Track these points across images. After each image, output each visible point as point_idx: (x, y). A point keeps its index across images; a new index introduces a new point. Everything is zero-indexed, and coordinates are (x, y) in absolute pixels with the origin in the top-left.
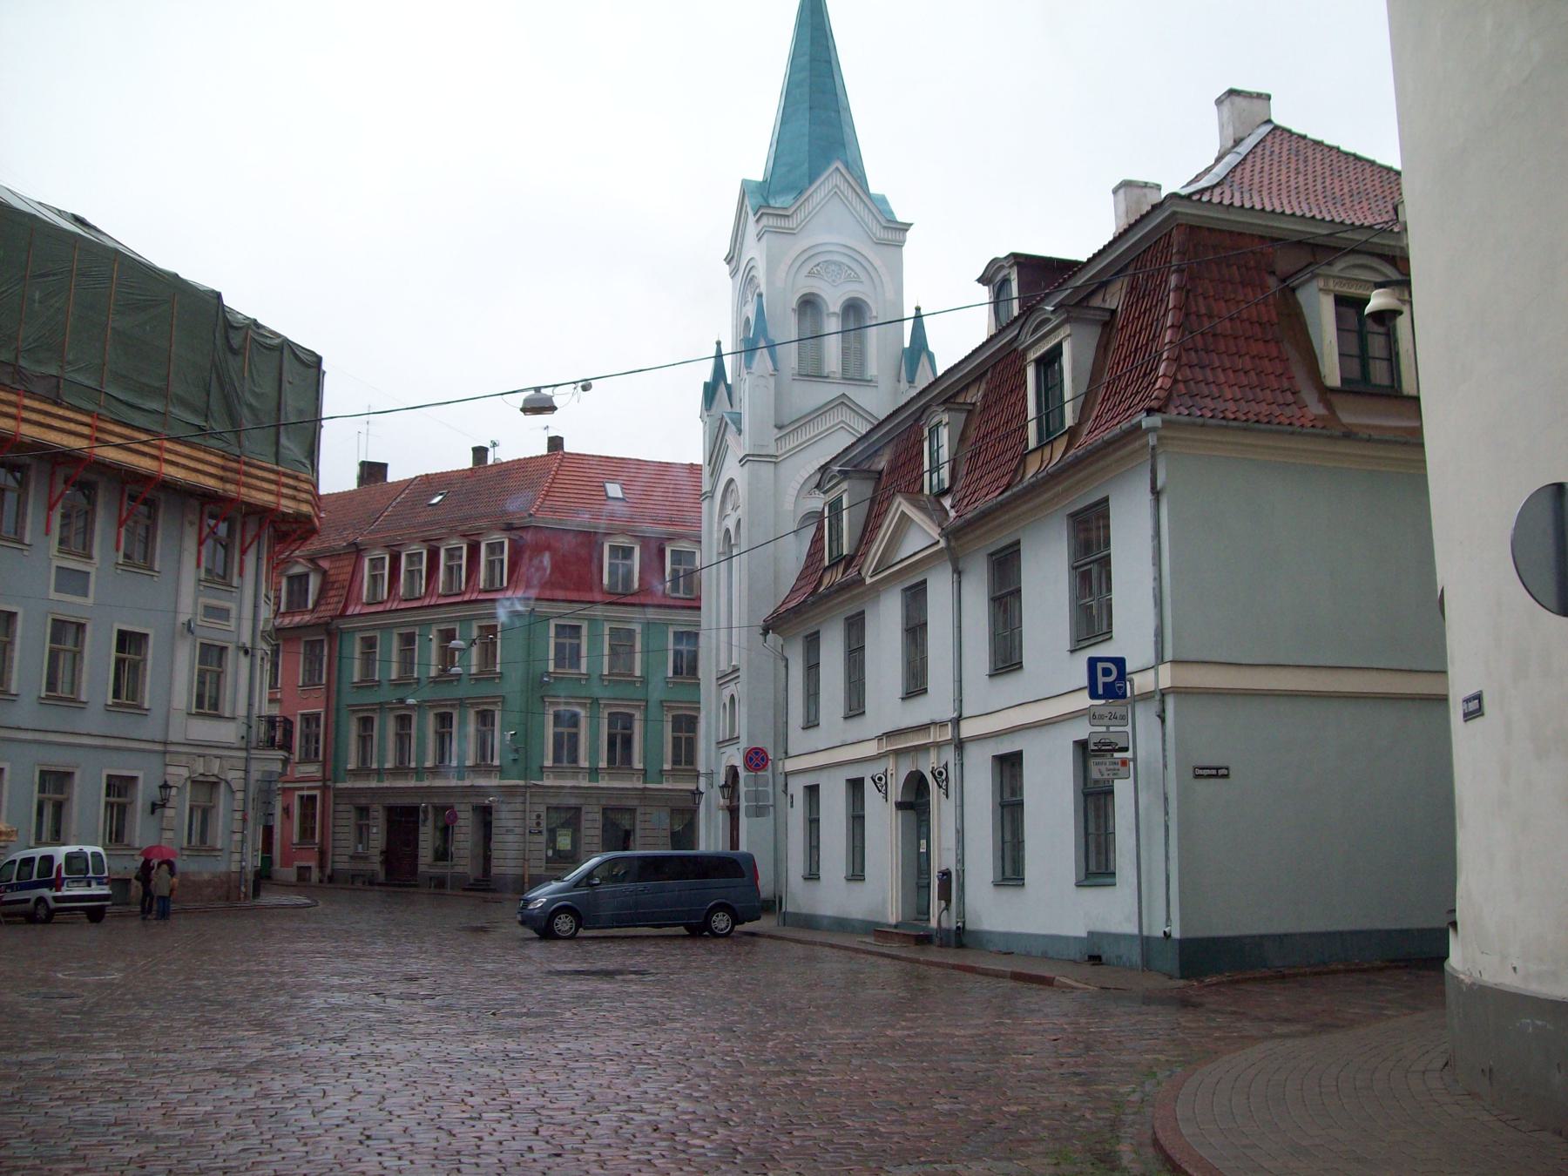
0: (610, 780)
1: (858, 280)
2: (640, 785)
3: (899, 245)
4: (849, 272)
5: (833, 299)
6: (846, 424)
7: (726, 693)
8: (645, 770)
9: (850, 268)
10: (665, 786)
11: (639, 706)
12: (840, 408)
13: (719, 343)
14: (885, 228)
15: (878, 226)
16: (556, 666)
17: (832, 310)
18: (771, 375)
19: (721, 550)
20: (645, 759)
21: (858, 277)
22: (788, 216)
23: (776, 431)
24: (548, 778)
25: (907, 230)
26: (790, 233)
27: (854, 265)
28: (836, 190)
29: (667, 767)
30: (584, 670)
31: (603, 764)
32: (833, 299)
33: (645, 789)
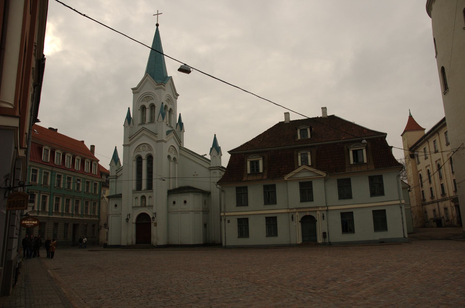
0: (41, 214)
2: (48, 216)
3: (177, 99)
7: (139, 195)
8: (49, 212)
10: (54, 216)
11: (49, 194)
13: (129, 108)
14: (176, 94)
16: (31, 181)
19: (134, 159)
20: (49, 209)
22: (165, 86)
24: (40, 214)
25: (178, 96)
26: (164, 90)
27: (171, 101)
29: (54, 211)
30: (38, 182)
31: (40, 210)
33: (49, 217)
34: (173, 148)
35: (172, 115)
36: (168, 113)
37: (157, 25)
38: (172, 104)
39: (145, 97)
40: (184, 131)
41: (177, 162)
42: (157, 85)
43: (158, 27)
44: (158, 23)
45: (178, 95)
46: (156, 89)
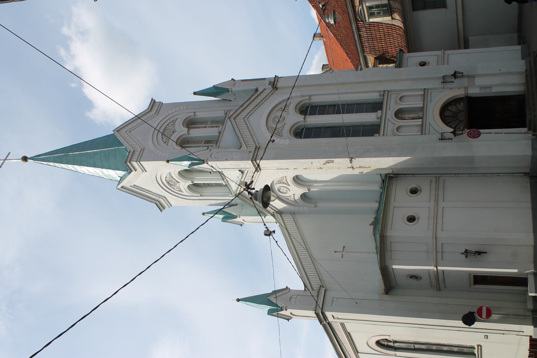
1: (174, 122)
3: (161, 104)
4: (170, 125)
5: (181, 130)
6: (246, 116)
9: (168, 124)
12: (236, 121)
14: (151, 110)
15: (150, 113)
17: (186, 132)
18: (210, 151)
19: (313, 206)
21: (174, 121)
22: (134, 151)
23: (242, 148)
25: (155, 101)
28: (128, 132)
32: (181, 130)
34: (272, 116)
35: (201, 115)
36: (196, 133)
37: (25, 159)
38: (175, 118)
39: (171, 187)
40: (232, 79)
41: (308, 97)
42: (136, 170)
43: (28, 157)
44: (21, 158)
45: (153, 103)
46: (144, 170)
